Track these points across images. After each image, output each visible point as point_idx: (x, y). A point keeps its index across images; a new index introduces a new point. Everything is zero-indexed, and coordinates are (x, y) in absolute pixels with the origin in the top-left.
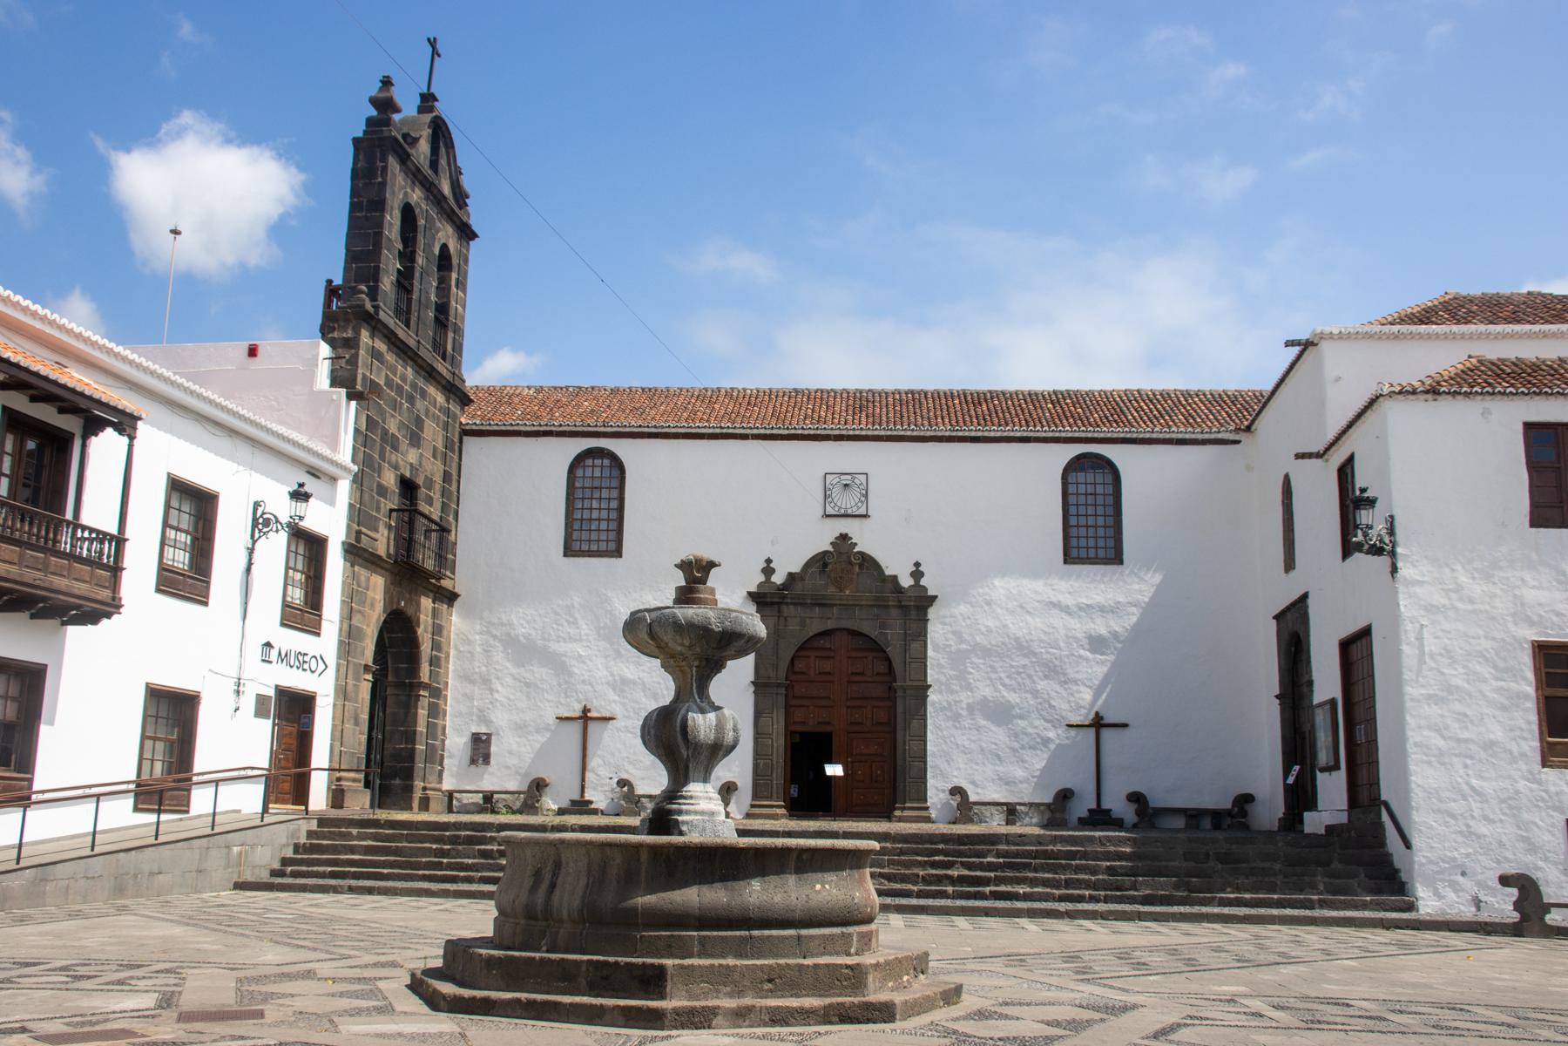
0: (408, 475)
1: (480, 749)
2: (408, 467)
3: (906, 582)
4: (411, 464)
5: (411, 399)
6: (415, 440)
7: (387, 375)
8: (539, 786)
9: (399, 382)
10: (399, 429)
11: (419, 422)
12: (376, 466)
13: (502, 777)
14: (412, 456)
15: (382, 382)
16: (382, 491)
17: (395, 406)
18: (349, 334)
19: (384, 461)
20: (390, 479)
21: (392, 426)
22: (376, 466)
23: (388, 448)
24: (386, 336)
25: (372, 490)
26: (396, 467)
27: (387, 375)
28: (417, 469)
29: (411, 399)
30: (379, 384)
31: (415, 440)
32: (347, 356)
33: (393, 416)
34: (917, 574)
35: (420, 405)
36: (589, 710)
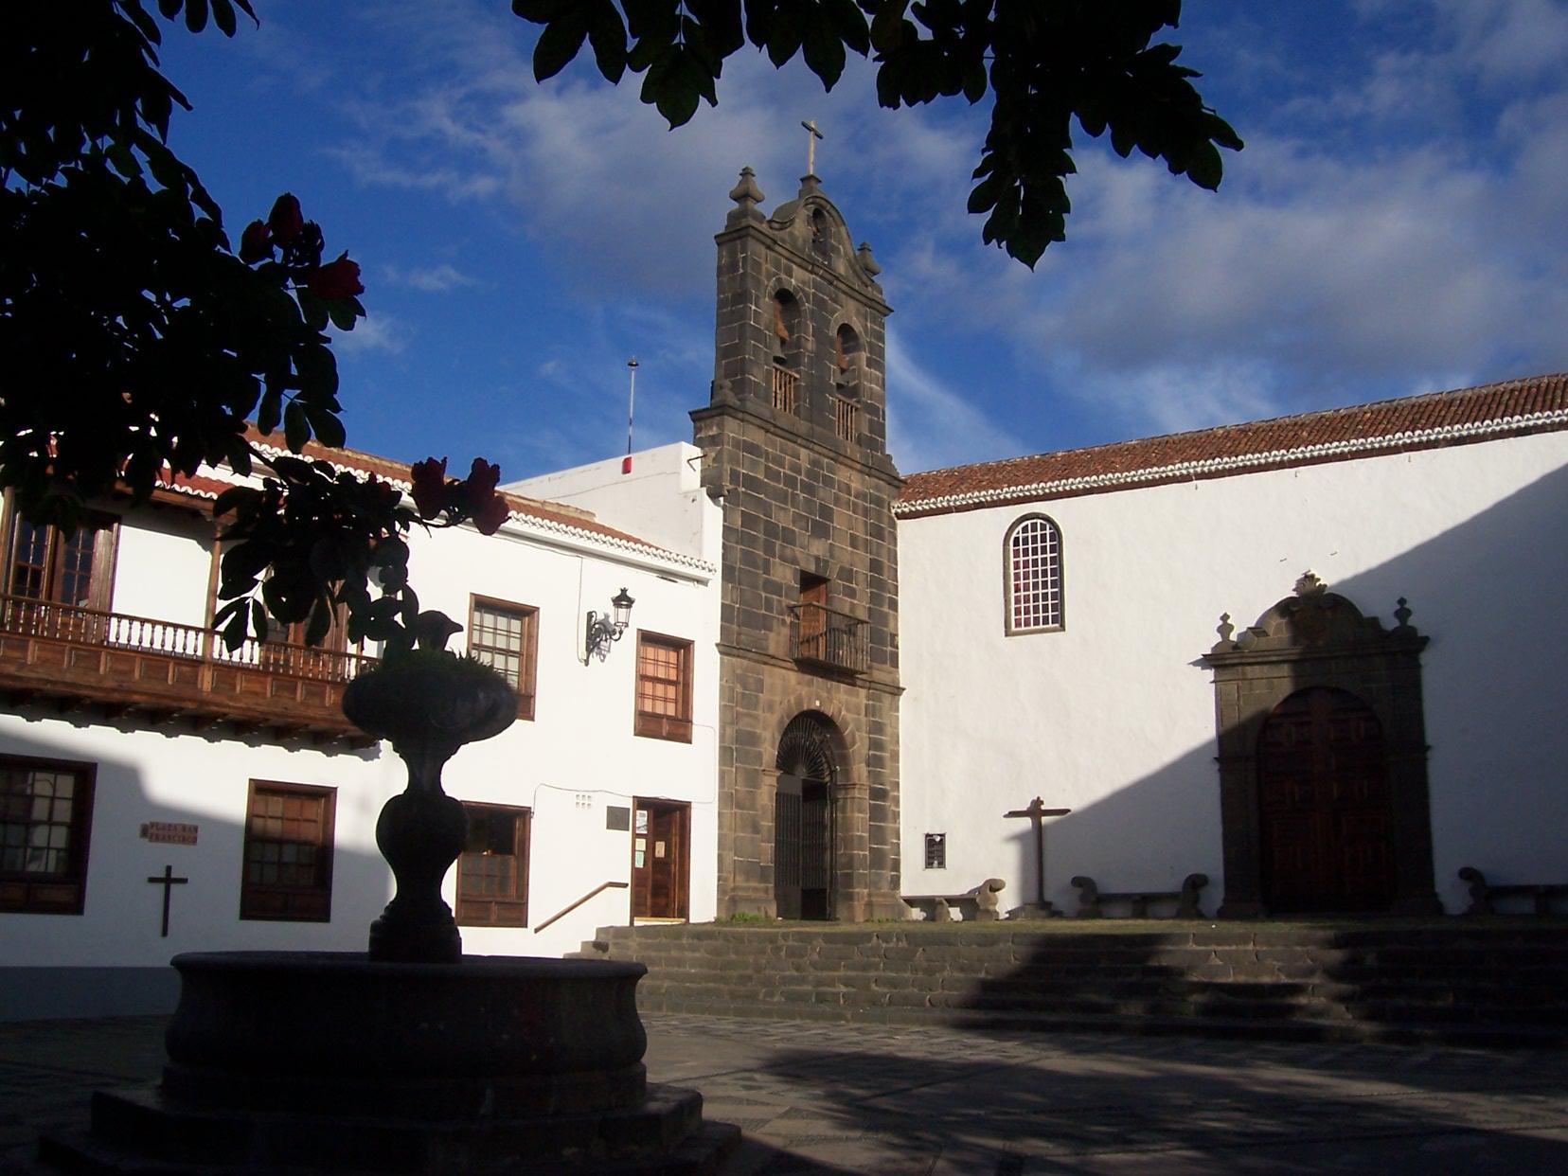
0: (812, 568)
1: (935, 850)
2: (813, 560)
3: (1390, 623)
4: (817, 559)
6: (821, 530)
7: (767, 468)
10: (794, 522)
11: (826, 513)
12: (760, 563)
13: (953, 881)
14: (818, 548)
15: (761, 477)
16: (775, 588)
17: (783, 498)
18: (714, 431)
19: (774, 556)
20: (784, 574)
21: (783, 519)
22: (760, 563)
23: (778, 543)
25: (757, 588)
27: (767, 468)
29: (809, 489)
31: (821, 530)
32: (713, 454)
34: (1403, 613)
35: (825, 495)
36: (1042, 803)
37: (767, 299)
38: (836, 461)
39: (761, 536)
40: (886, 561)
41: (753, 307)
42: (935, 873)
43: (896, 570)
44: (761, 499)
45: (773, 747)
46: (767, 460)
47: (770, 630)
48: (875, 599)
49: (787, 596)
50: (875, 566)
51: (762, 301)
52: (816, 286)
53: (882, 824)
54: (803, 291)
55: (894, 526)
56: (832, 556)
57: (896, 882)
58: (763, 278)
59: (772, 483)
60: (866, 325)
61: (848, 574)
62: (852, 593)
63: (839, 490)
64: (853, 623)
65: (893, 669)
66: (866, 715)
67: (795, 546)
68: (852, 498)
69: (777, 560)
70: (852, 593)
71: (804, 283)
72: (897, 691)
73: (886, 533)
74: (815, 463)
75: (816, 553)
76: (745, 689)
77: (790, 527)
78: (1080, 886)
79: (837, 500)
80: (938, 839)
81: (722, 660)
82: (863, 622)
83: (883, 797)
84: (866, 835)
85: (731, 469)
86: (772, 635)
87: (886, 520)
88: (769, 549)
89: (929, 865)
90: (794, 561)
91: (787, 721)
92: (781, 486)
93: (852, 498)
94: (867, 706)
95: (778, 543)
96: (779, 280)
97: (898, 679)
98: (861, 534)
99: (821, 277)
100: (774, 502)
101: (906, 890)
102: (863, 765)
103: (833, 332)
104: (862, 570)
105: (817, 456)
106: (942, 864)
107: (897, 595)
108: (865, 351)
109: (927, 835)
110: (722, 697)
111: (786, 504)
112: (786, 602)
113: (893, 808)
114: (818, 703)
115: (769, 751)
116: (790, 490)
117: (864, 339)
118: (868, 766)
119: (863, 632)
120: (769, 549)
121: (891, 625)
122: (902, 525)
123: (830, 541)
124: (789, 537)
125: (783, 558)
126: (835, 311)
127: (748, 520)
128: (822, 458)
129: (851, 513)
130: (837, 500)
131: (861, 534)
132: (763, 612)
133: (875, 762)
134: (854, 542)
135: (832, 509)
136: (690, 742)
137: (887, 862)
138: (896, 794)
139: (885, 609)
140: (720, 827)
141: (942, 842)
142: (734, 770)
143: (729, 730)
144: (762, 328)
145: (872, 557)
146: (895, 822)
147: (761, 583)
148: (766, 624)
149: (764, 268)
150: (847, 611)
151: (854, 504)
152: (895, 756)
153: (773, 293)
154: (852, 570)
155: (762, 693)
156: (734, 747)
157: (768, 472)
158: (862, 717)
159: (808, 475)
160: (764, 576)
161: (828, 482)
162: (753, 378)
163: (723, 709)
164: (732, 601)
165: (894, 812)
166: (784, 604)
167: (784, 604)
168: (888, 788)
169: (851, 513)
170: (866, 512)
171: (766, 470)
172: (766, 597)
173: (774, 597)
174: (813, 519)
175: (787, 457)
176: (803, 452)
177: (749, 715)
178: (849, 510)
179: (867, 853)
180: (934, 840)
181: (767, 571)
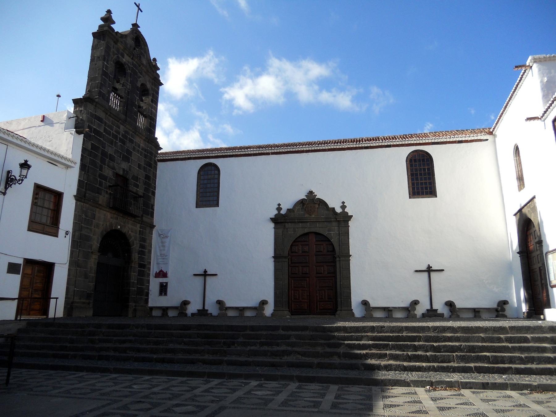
0: (121, 173)
1: (163, 289)
4: (124, 170)
5: (124, 143)
6: (126, 159)
7: (105, 129)
8: (185, 303)
9: (115, 133)
14: (124, 165)
15: (102, 131)
17: (112, 143)
19: (105, 165)
21: (110, 151)
24: (103, 111)
26: (113, 168)
28: (128, 172)
29: (124, 143)
30: (100, 132)
31: (126, 159)
33: (110, 146)
35: (128, 144)
37: (112, 62)
38: (135, 133)
39: (100, 155)
40: (152, 177)
41: (106, 63)
42: (163, 298)
43: (156, 181)
44: (102, 140)
46: (105, 125)
47: (101, 194)
48: (146, 190)
49: (109, 182)
50: (147, 177)
51: (109, 62)
52: (133, 64)
53: (143, 278)
54: (128, 65)
55: (156, 165)
56: (130, 170)
57: (147, 301)
58: (111, 54)
59: (106, 135)
60: (152, 87)
61: (136, 178)
62: (137, 186)
64: (137, 197)
65: (151, 218)
66: (139, 235)
67: (115, 162)
68: (140, 150)
69: (106, 166)
70: (137, 186)
71: (128, 62)
72: (152, 227)
73: (153, 166)
74: (126, 132)
75: (123, 167)
76: (86, 216)
77: (113, 154)
78: (219, 304)
79: (134, 149)
80: (165, 284)
81: (76, 203)
82: (140, 197)
83: (144, 266)
84: (136, 282)
85: (88, 125)
86: (101, 197)
87: (153, 161)
88: (103, 162)
89: (161, 294)
90: (113, 168)
91: (105, 233)
92: (111, 137)
93: (140, 150)
94: (140, 231)
95: (107, 160)
96: (118, 57)
97: (153, 222)
98: (142, 164)
99: (136, 62)
100: (106, 143)
101: (150, 304)
102: (137, 254)
103: (139, 85)
104: (142, 177)
105: (127, 130)
106: (166, 294)
107: (155, 190)
108: (151, 96)
109: (161, 283)
111: (112, 145)
112: (108, 184)
113: (148, 272)
114: (119, 227)
115: (96, 244)
116: (115, 140)
117: (151, 92)
119: (141, 201)
120: (103, 162)
121: (152, 200)
122: (159, 164)
123: (130, 164)
124: (112, 158)
125: (109, 166)
126: (140, 77)
127: (94, 147)
128: (129, 131)
129: (139, 155)
130: (134, 149)
131: (142, 164)
132: (98, 186)
133: (141, 253)
134: (139, 166)
135: (132, 152)
136: (57, 236)
137: (144, 293)
138: (149, 266)
139: (150, 194)
140: (69, 275)
141: (166, 286)
142: (78, 250)
143: (77, 234)
144: (109, 73)
145: (146, 173)
146: (148, 277)
147: (98, 174)
148: (99, 192)
149: (112, 50)
150: (135, 191)
151: (141, 152)
152: (150, 251)
153: (115, 61)
154: (138, 177)
156: (79, 241)
157: (105, 130)
158: (138, 235)
159: (122, 136)
160: (100, 171)
161: (131, 141)
162: (102, 91)
164: (83, 179)
165: (148, 273)
167: (107, 185)
168: (146, 263)
169: (139, 155)
170: (146, 156)
171: (104, 130)
172: (100, 181)
173: (104, 181)
174: (124, 155)
175: (114, 127)
176: (122, 127)
177: (87, 228)
178: (139, 154)
179: (136, 289)
180: (163, 285)
181: (101, 170)
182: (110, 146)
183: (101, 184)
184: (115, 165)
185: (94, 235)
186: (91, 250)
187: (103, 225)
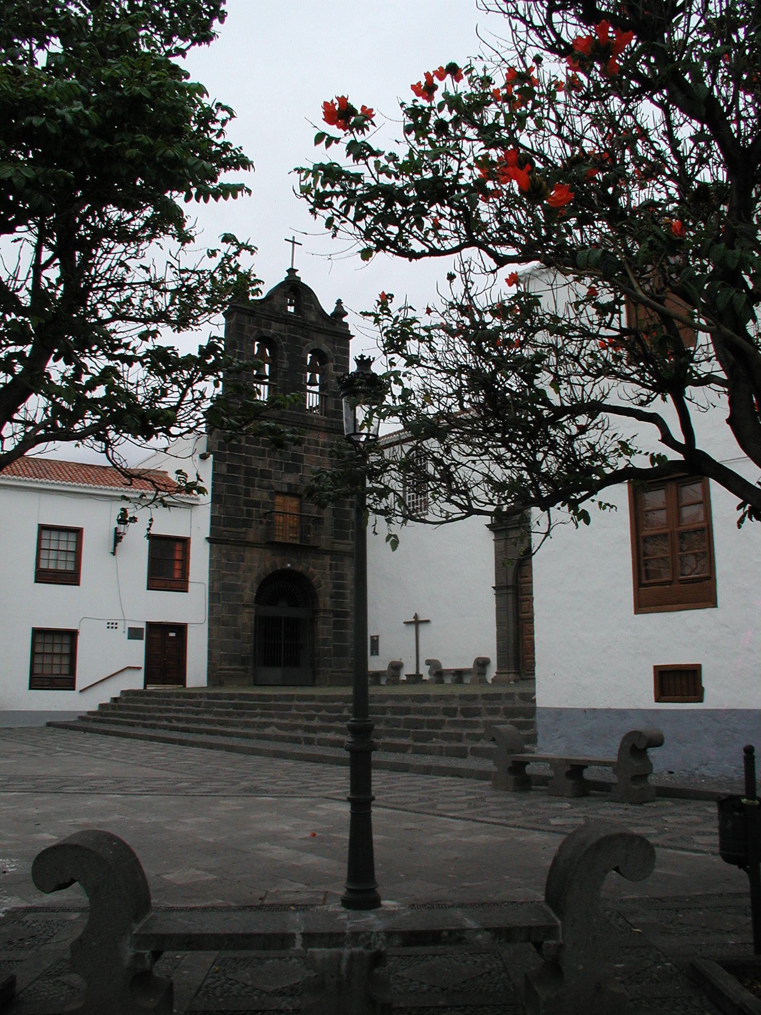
4: (289, 485)
21: (260, 465)
33: (260, 459)
39: (242, 476)
45: (252, 591)
63: (309, 444)
81: (211, 548)
91: (264, 577)
94: (331, 564)
95: (257, 479)
102: (328, 598)
110: (210, 567)
115: (249, 593)
118: (332, 598)
124: (265, 475)
127: (231, 468)
130: (307, 450)
143: (216, 584)
148: (247, 524)
155: (243, 562)
158: (328, 571)
163: (211, 573)
166: (261, 512)
167: (261, 512)
182: (260, 459)
183: (249, 514)
184: (273, 482)
185: (244, 582)
186: (243, 601)
187: (259, 567)
